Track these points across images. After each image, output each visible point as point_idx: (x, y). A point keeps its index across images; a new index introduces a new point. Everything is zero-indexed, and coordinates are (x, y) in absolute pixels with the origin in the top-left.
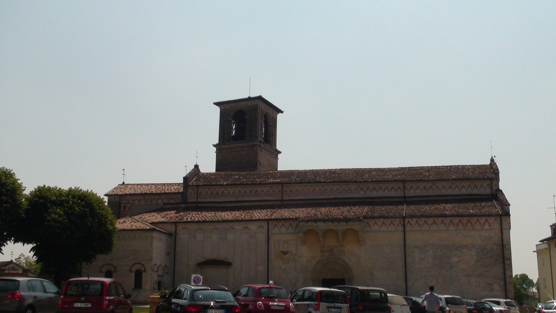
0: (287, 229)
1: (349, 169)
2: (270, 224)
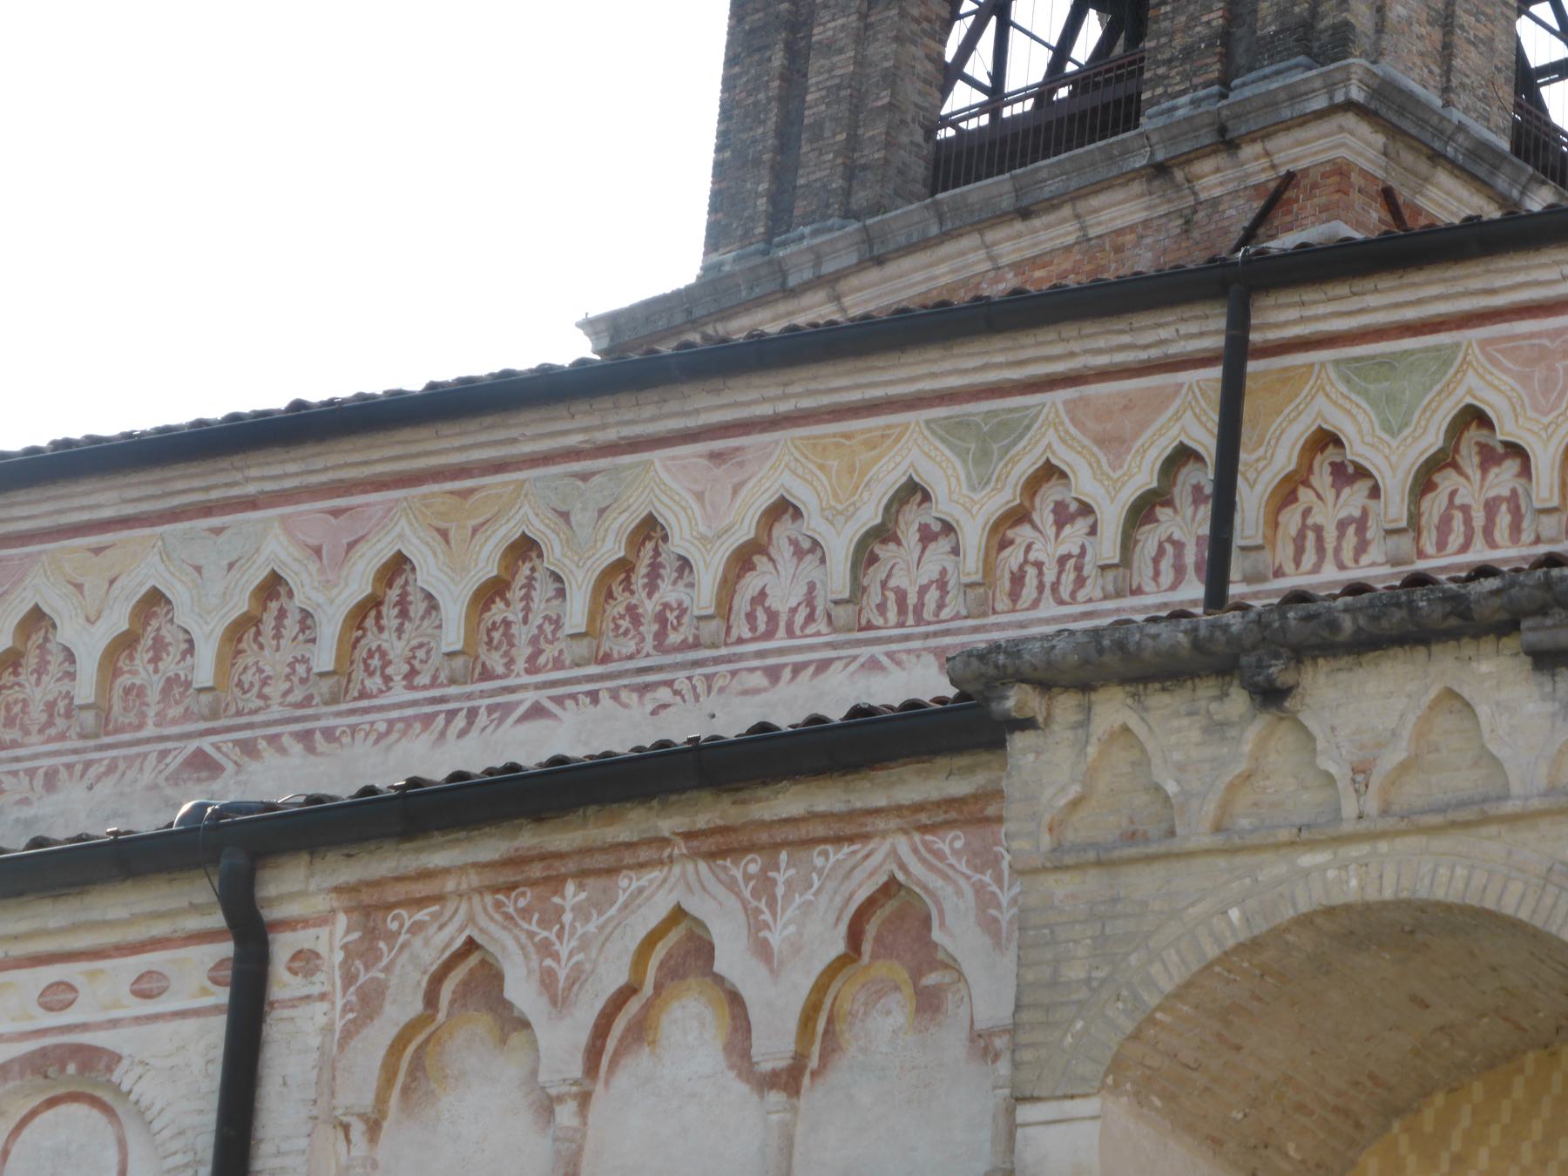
0: (789, 1080)
2: (305, 961)
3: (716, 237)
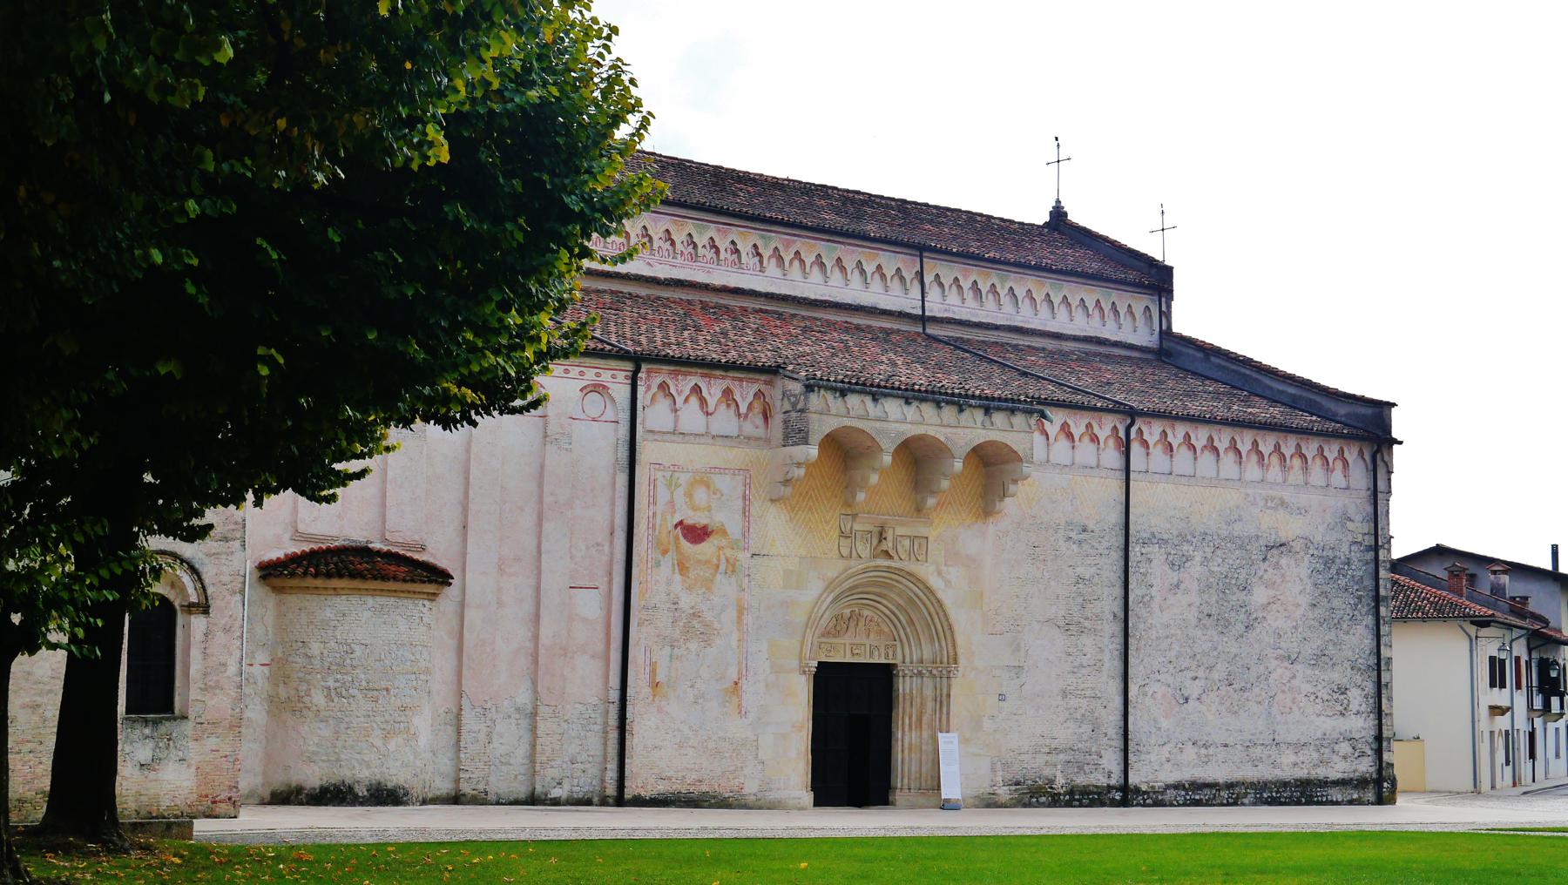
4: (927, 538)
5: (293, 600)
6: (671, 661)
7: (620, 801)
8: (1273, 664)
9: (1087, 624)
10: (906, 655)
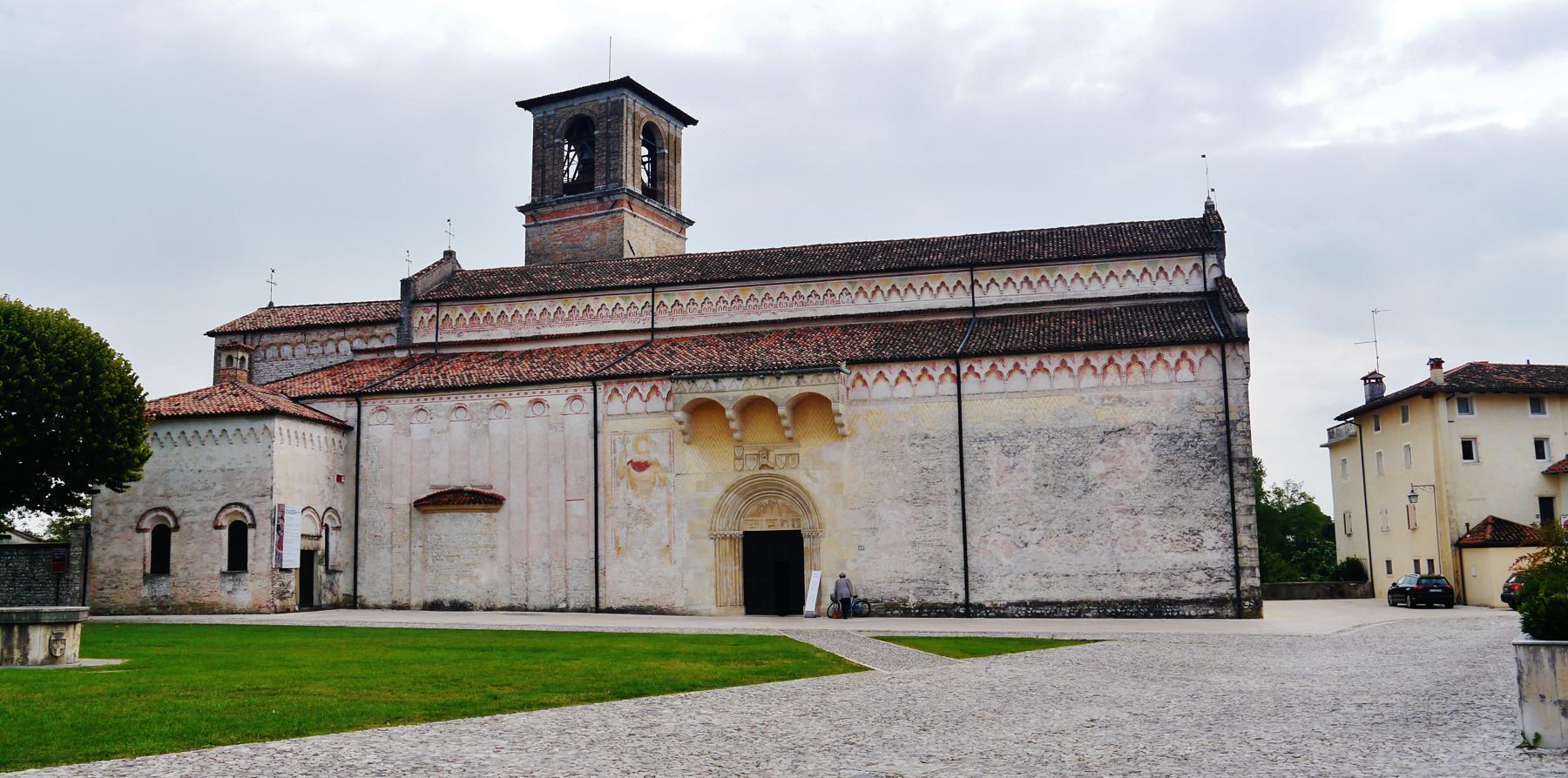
1: (838, 244)
2: (600, 389)
3: (533, 195)
4: (798, 454)
5: (428, 516)
6: (627, 535)
7: (597, 610)
8: (1115, 516)
9: (931, 498)
10: (804, 526)
